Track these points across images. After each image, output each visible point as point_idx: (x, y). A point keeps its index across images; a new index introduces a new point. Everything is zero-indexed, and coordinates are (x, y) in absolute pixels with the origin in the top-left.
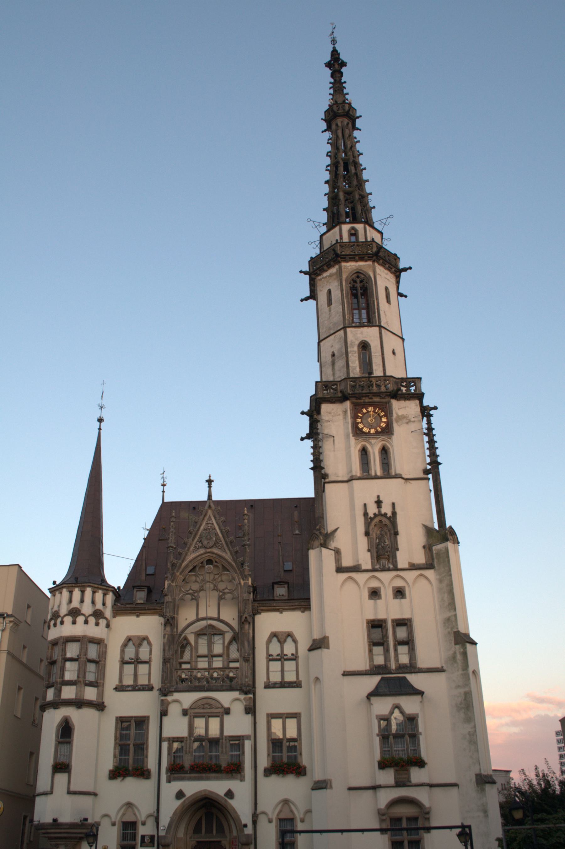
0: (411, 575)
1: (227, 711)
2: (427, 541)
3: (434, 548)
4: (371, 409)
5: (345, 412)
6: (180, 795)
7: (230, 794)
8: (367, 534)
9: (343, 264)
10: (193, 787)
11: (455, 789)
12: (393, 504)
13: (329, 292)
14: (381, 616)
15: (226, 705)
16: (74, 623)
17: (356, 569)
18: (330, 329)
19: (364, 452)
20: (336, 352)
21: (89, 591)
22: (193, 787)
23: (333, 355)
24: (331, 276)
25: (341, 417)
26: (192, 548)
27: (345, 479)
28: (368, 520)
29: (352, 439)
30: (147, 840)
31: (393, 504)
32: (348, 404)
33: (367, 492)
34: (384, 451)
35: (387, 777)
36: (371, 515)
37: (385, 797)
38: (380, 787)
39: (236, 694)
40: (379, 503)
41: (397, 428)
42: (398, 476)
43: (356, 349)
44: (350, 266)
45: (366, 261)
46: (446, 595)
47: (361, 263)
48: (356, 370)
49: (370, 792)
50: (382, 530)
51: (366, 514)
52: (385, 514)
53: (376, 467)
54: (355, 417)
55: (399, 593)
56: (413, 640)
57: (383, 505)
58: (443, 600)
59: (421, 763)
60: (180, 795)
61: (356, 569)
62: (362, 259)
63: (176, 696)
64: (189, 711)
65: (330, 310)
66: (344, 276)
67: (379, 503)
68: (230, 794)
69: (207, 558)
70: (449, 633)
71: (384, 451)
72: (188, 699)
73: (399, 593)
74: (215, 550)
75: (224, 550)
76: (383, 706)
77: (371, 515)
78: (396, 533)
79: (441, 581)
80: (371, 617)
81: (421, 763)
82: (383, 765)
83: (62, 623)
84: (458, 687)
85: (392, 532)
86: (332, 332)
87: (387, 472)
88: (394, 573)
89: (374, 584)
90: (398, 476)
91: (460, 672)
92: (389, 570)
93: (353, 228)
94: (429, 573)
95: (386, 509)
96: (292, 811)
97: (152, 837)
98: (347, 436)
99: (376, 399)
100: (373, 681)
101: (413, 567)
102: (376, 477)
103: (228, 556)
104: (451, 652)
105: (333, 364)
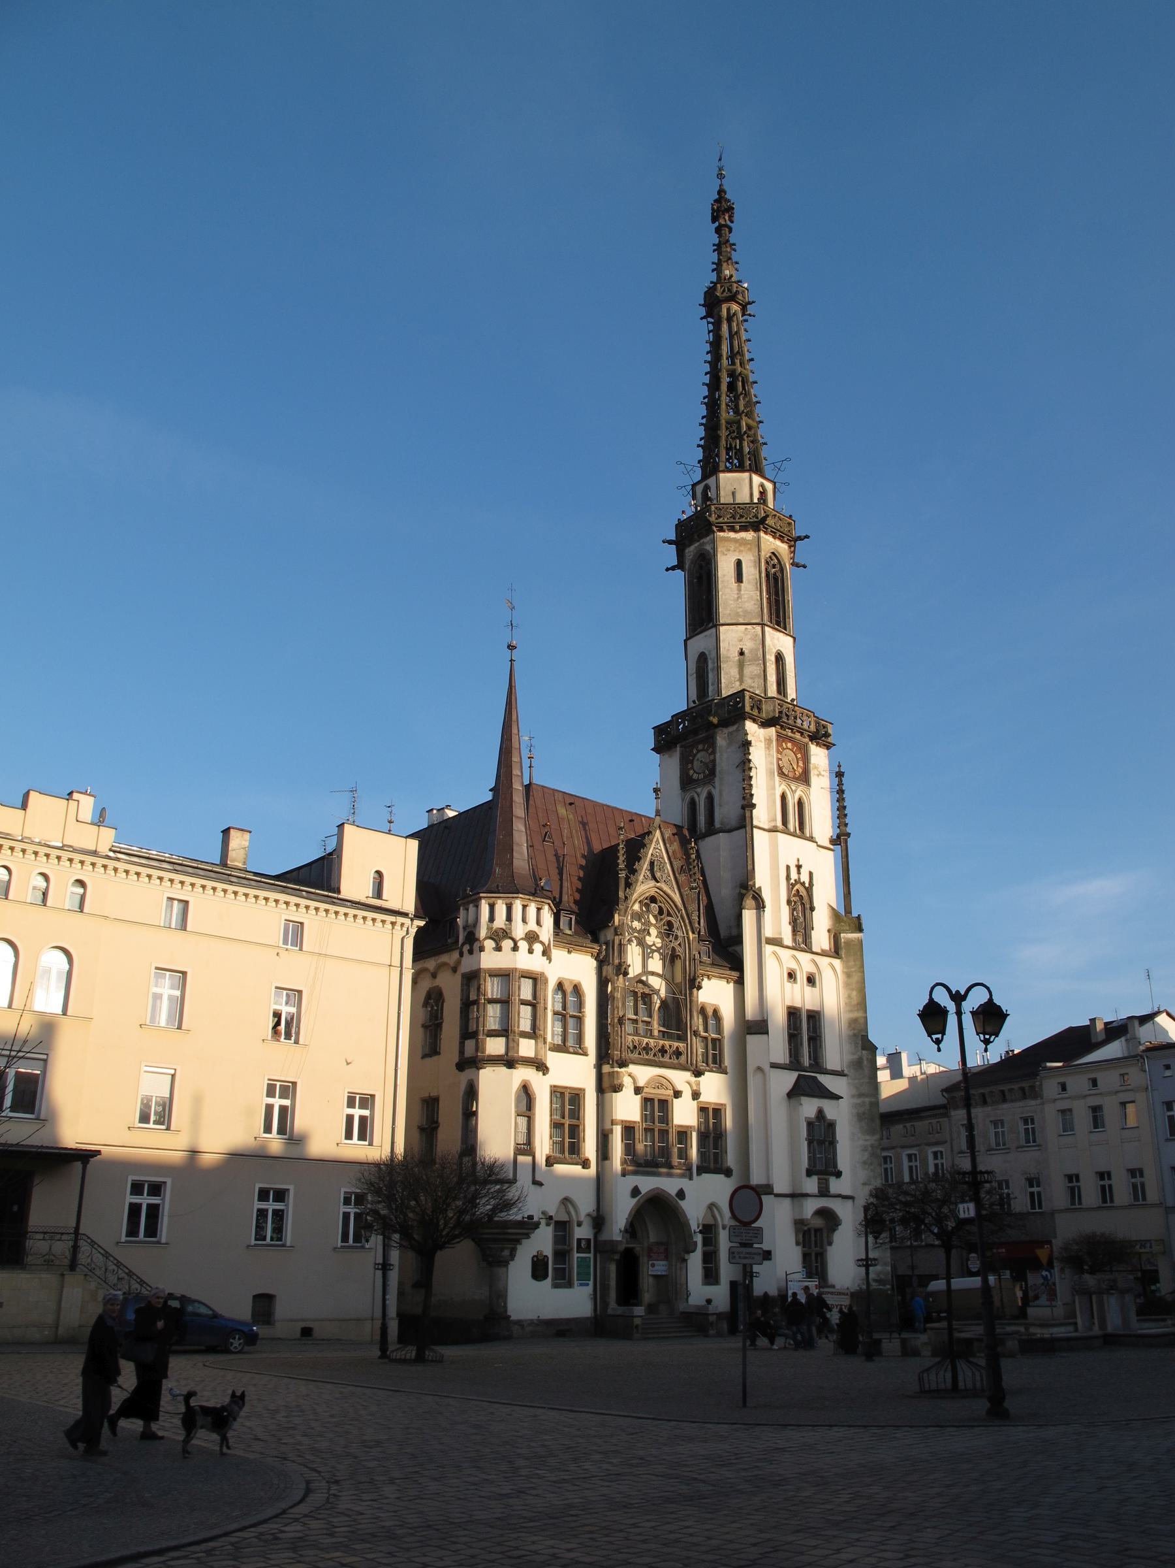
0: (824, 962)
1: (677, 1094)
2: (834, 925)
3: (842, 935)
4: (789, 745)
5: (768, 741)
6: (635, 1192)
7: (681, 1194)
8: (789, 902)
9: (762, 534)
10: (647, 1184)
11: (850, 1201)
12: (811, 874)
13: (739, 564)
14: (798, 1004)
15: (679, 1088)
16: (531, 951)
17: (777, 942)
18: (738, 615)
19: (783, 797)
20: (746, 652)
21: (518, 906)
22: (647, 1184)
23: (742, 653)
24: (743, 542)
25: (763, 745)
26: (641, 877)
27: (766, 827)
28: (791, 886)
29: (777, 778)
30: (583, 1244)
31: (811, 874)
32: (772, 731)
33: (791, 849)
34: (800, 804)
35: (811, 1185)
36: (792, 881)
37: (810, 1207)
38: (807, 1195)
39: (687, 1075)
40: (799, 867)
41: (814, 779)
42: (811, 839)
43: (773, 659)
44: (770, 543)
45: (783, 542)
46: (854, 993)
47: (778, 543)
48: (772, 691)
49: (788, 1201)
50: (801, 901)
51: (788, 877)
52: (803, 884)
53: (793, 823)
54: (778, 752)
55: (811, 980)
56: (820, 1037)
57: (802, 870)
58: (849, 997)
59: (838, 1174)
60: (635, 1192)
61: (777, 942)
62: (781, 539)
63: (632, 1068)
64: (646, 1090)
65: (739, 590)
66: (763, 554)
67: (799, 867)
68: (681, 1194)
69: (652, 893)
70: (855, 1035)
71: (800, 804)
72: (643, 1074)
73: (811, 980)
74: (665, 888)
75: (672, 888)
76: (809, 1107)
77: (792, 881)
78: (812, 909)
79: (848, 975)
80: (790, 1004)
81: (838, 1174)
82: (809, 1173)
83: (515, 948)
84: (860, 1095)
85: (808, 906)
86: (741, 621)
87: (802, 831)
88: (809, 956)
89: (793, 965)
90: (811, 839)
91: (866, 1080)
92: (803, 950)
93: (762, 485)
94: (837, 963)
95: (805, 878)
96: (714, 1216)
97: (588, 1241)
98: (771, 773)
99: (798, 736)
100: (790, 1078)
101: (823, 954)
102: (794, 835)
103: (677, 898)
104: (856, 1057)
105: (741, 666)
